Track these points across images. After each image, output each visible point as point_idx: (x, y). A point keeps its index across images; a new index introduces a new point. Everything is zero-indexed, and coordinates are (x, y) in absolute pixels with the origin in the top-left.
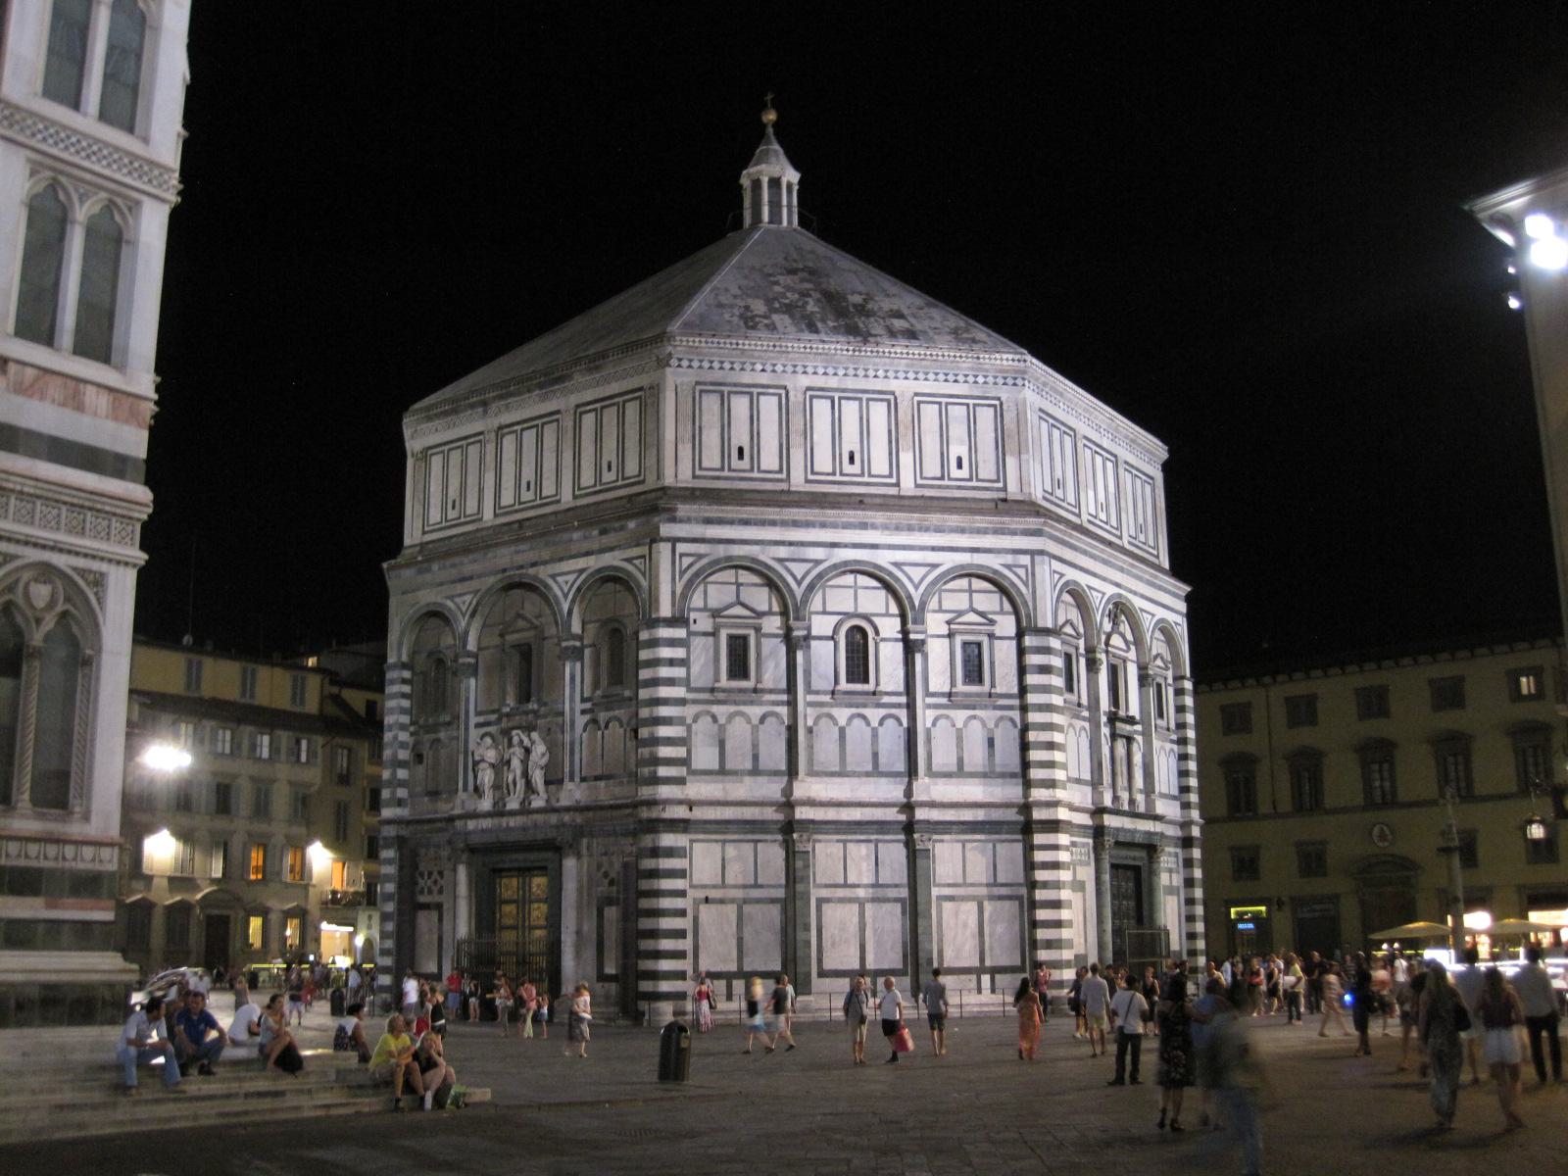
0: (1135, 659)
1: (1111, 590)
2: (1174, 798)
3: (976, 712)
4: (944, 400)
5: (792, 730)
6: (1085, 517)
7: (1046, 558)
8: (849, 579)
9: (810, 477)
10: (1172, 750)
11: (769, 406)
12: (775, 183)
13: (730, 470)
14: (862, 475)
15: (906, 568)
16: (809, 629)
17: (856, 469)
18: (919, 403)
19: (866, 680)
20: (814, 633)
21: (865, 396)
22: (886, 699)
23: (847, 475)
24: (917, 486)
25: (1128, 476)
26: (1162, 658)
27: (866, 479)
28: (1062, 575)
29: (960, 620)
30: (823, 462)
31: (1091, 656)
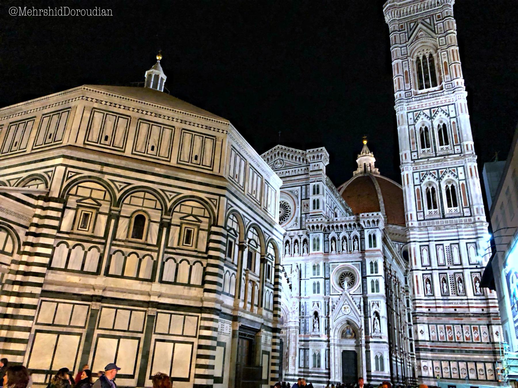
0: (260, 252)
1: (253, 221)
2: (271, 311)
6: (246, 193)
7: (225, 199)
8: (142, 194)
10: (271, 292)
12: (157, 77)
14: (156, 155)
15: (165, 192)
17: (154, 153)
18: (184, 132)
21: (162, 126)
24: (178, 163)
25: (266, 185)
26: (271, 255)
27: (157, 157)
29: (187, 218)
31: (241, 244)
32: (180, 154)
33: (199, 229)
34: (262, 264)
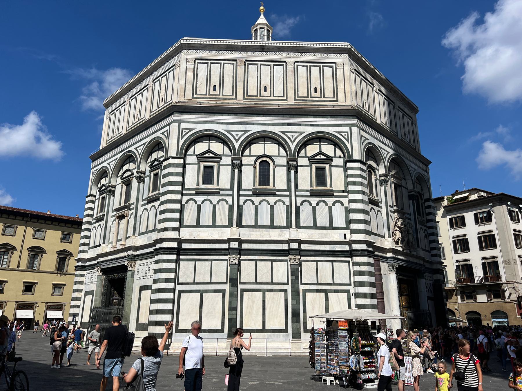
3: (323, 199)
5: (231, 208)
9: (246, 97)
11: (229, 68)
13: (210, 95)
14: (270, 96)
16: (241, 161)
18: (298, 66)
19: (269, 185)
20: (243, 163)
22: (278, 193)
23: (263, 96)
24: (295, 100)
27: (272, 98)
28: (367, 139)
30: (252, 91)
32: (296, 90)
33: (331, 166)
34: (411, 202)
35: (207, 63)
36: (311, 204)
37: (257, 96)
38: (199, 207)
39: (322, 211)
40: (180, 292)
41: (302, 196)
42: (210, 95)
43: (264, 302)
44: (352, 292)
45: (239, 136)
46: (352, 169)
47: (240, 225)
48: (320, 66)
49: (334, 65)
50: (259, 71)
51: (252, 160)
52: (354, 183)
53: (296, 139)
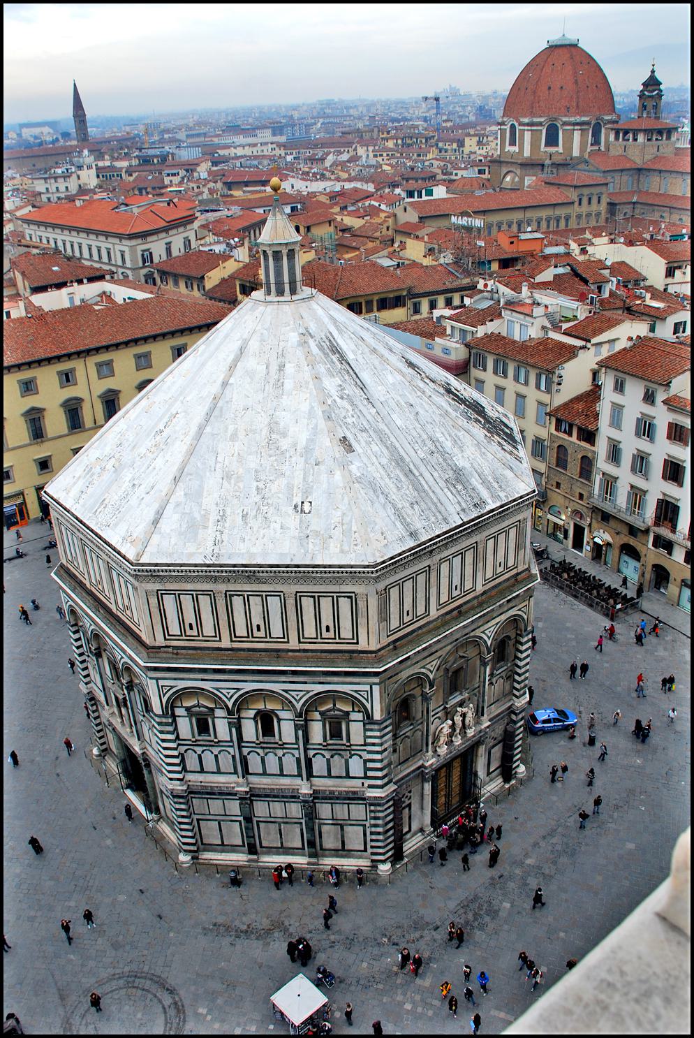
3: (340, 752)
4: (316, 595)
9: (234, 639)
11: (205, 602)
18: (300, 596)
24: (300, 642)
27: (268, 639)
30: (241, 631)
35: (175, 594)
36: (324, 757)
37: (248, 637)
38: (200, 756)
39: (338, 763)
40: (198, 820)
41: (314, 749)
42: (186, 636)
43: (280, 830)
44: (368, 825)
45: (230, 694)
46: (371, 730)
47: (246, 772)
48: (333, 597)
49: (353, 595)
50: (247, 603)
51: (252, 713)
52: (374, 744)
53: (301, 698)
